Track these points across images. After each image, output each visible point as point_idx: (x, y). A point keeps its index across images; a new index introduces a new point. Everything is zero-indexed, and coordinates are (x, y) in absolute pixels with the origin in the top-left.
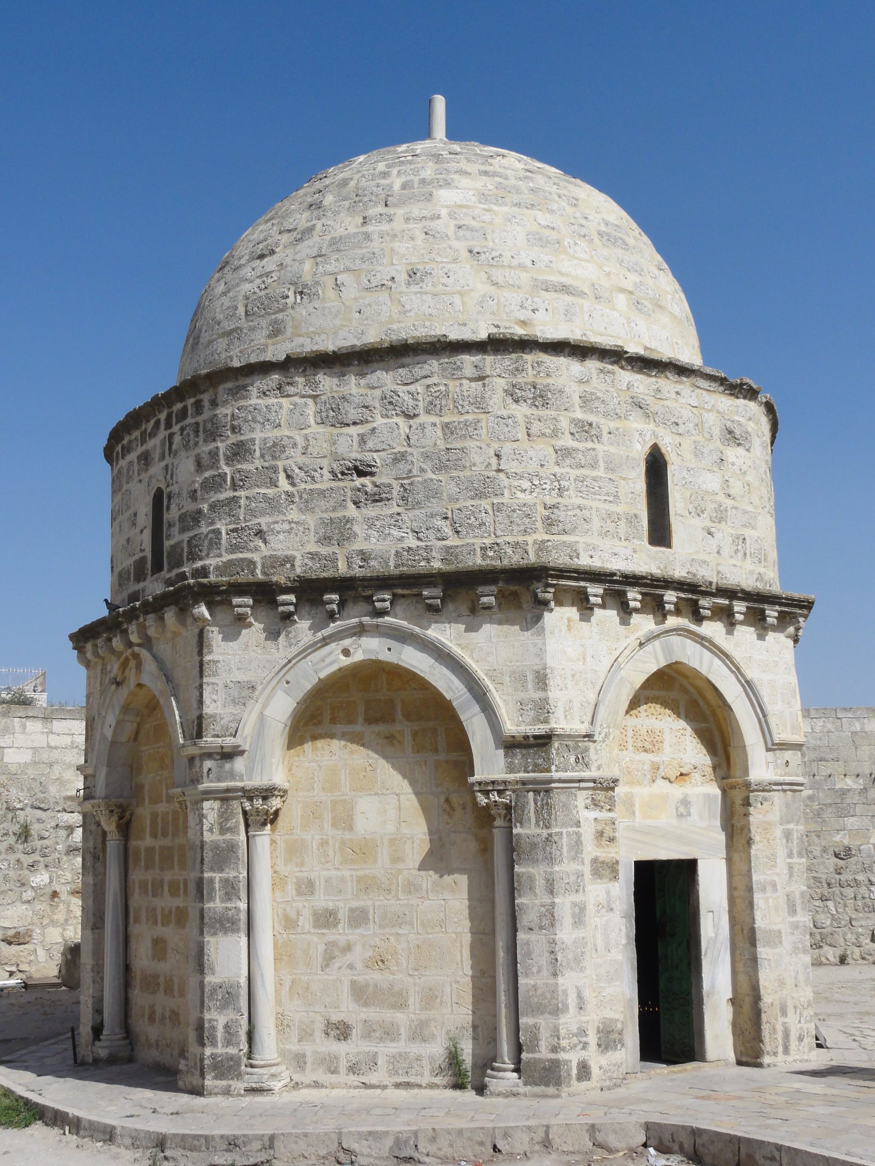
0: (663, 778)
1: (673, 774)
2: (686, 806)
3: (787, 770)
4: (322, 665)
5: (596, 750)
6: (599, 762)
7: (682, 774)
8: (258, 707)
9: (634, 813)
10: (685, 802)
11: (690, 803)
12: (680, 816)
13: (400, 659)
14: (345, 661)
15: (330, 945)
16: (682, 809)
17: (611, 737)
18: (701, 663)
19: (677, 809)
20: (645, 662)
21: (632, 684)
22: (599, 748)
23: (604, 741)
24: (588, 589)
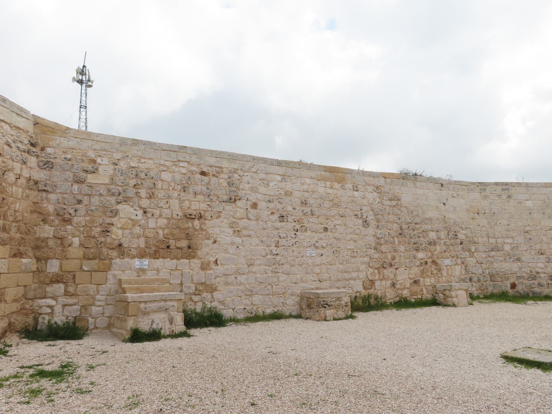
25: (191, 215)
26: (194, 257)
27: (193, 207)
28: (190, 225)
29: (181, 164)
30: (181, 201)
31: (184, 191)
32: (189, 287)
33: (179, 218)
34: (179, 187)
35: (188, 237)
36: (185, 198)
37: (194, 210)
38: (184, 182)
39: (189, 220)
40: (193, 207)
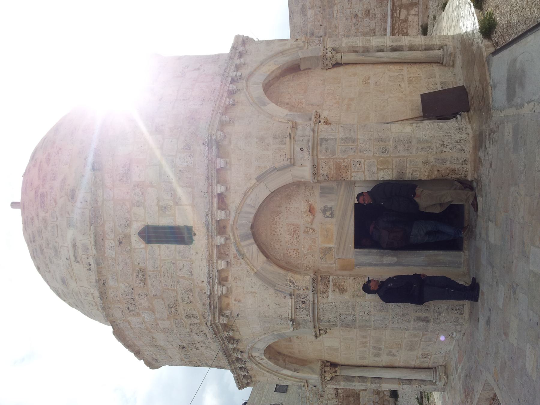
0: (312, 224)
1: (309, 218)
2: (326, 211)
3: (305, 149)
4: (268, 364)
5: (299, 289)
6: (304, 288)
7: (310, 211)
8: (288, 378)
9: (330, 248)
10: (324, 211)
11: (325, 207)
12: (332, 215)
13: (263, 349)
14: (266, 360)
15: (387, 355)
16: (328, 214)
17: (291, 279)
18: (250, 213)
19: (328, 217)
20: (253, 253)
21: (264, 262)
22: (297, 288)
23: (294, 284)
24: (219, 295)
25: (336, 395)
26: (359, 395)
27: (332, 392)
28: (341, 395)
29: (308, 395)
30: (329, 399)
31: (323, 397)
32: (376, 398)
33: (337, 401)
34: (321, 399)
35: (348, 396)
36: (327, 397)
37: (333, 392)
38: (318, 396)
39: (339, 395)
40: (332, 392)
